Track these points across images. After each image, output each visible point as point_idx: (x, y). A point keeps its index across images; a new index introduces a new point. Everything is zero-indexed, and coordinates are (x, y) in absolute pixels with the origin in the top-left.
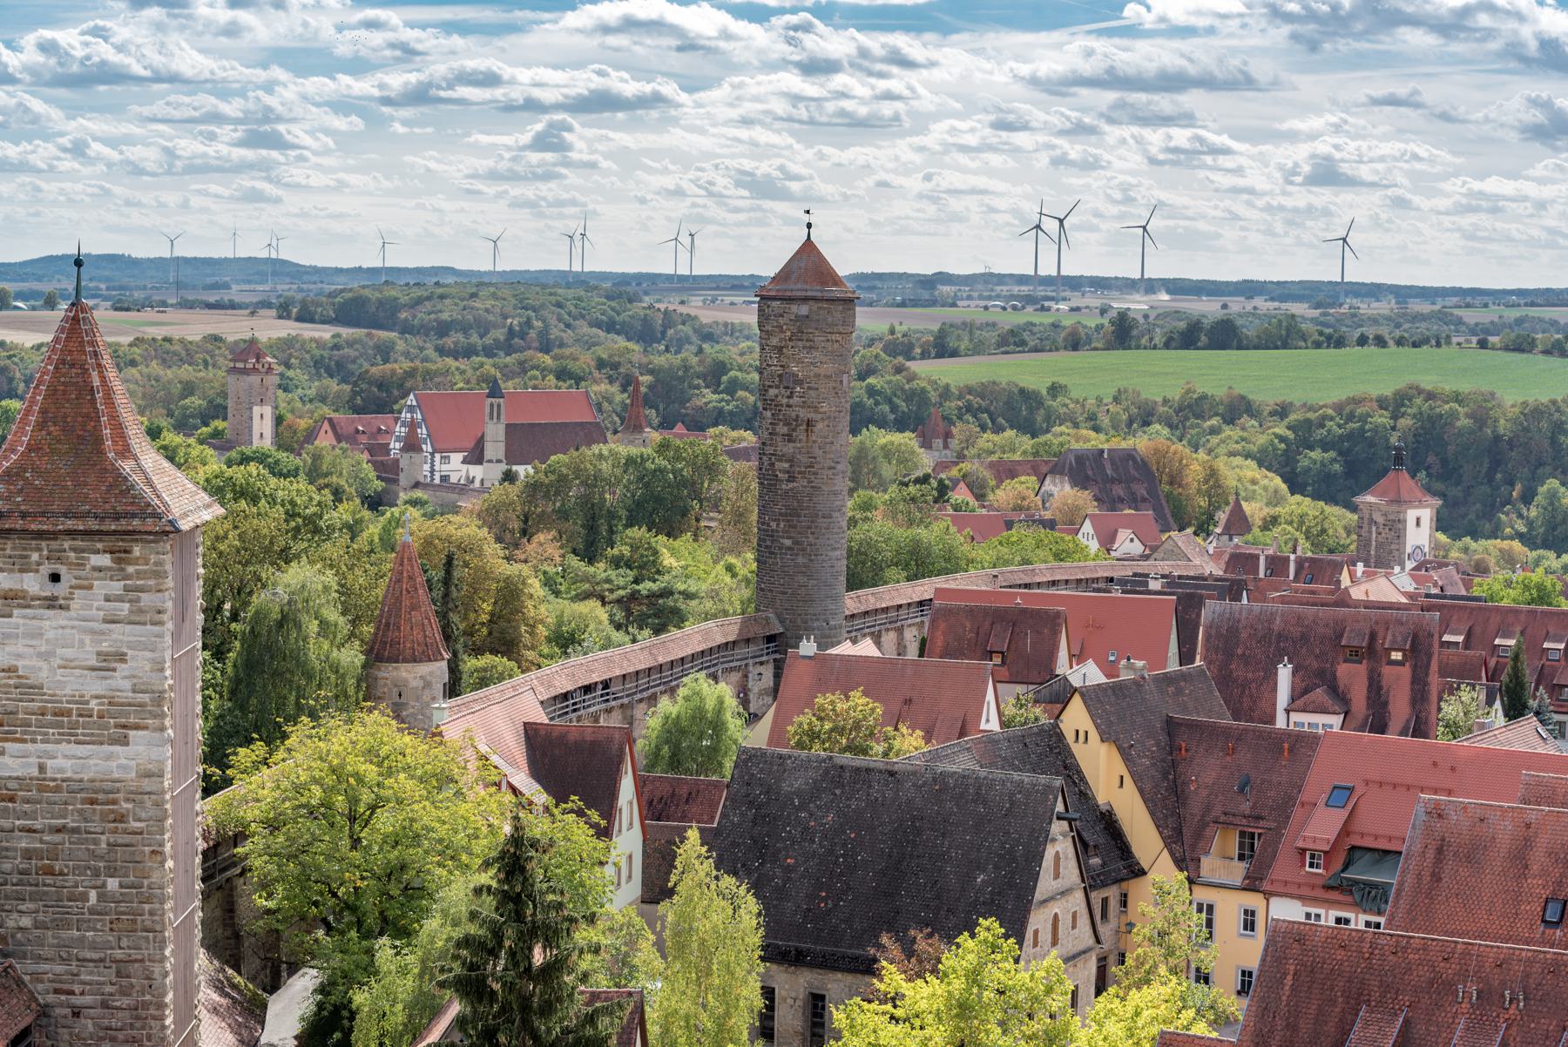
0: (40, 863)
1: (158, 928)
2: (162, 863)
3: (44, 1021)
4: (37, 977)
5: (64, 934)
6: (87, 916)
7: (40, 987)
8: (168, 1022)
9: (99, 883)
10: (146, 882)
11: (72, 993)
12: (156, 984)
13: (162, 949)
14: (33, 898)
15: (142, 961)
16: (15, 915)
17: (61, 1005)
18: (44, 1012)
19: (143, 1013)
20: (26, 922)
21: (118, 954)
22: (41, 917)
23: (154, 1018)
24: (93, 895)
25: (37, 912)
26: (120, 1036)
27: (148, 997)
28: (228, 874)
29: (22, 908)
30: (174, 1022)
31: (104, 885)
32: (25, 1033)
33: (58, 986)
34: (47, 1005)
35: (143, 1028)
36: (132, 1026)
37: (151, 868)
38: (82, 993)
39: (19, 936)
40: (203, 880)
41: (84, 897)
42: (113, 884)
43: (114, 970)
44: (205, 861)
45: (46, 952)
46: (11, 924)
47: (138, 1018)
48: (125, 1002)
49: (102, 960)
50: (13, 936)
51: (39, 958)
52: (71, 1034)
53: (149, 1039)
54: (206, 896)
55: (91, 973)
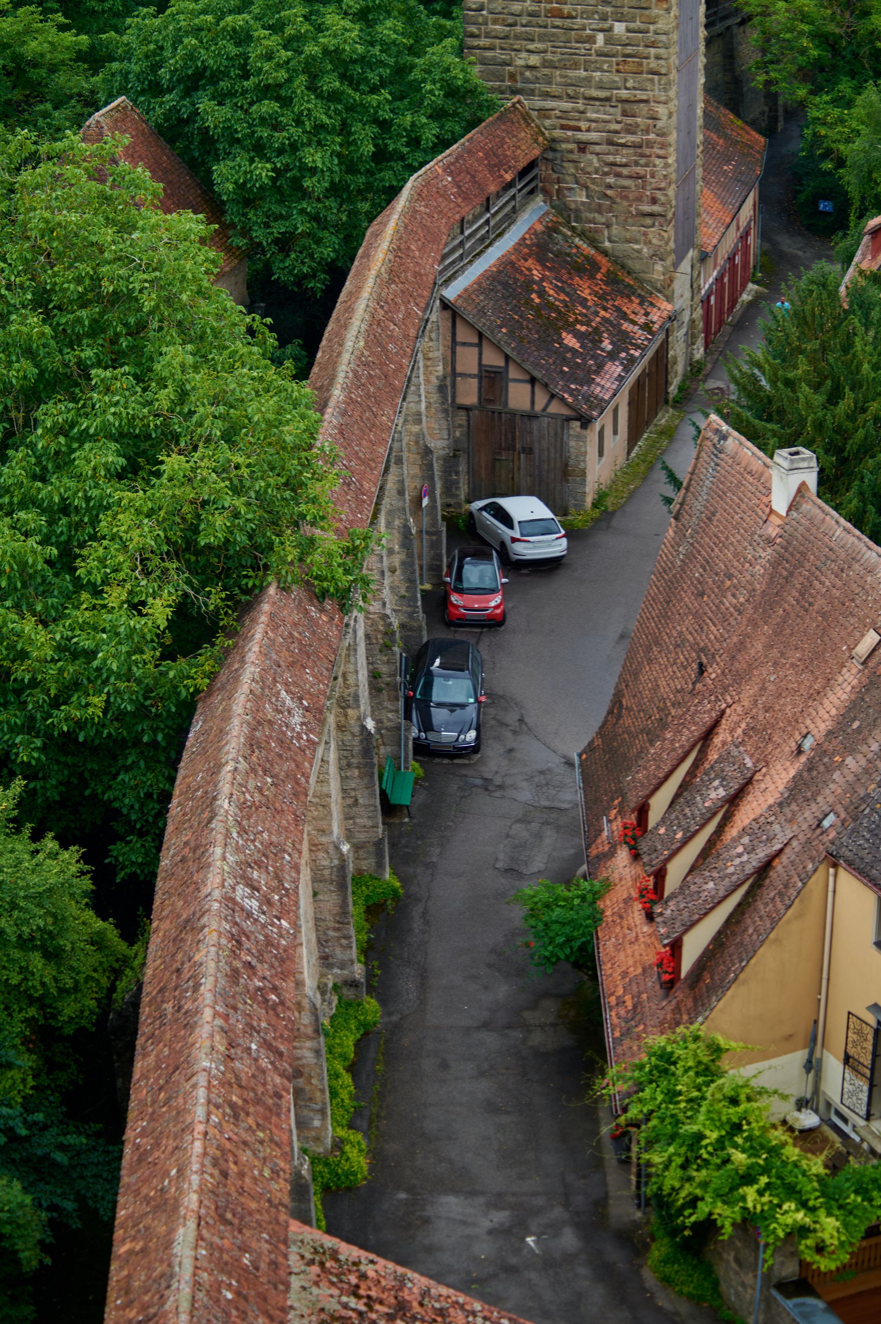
0: (548, 6)
1: (663, 71)
2: (668, 10)
3: (550, 155)
4: (544, 113)
5: (570, 73)
6: (594, 58)
7: (548, 123)
8: (670, 161)
9: (606, 26)
10: (652, 27)
11: (578, 129)
12: (660, 124)
13: (665, 90)
14: (542, 38)
15: (646, 101)
16: (524, 55)
17: (567, 140)
18: (552, 145)
19: (647, 151)
20: (534, 60)
21: (624, 93)
22: (549, 56)
23: (659, 157)
24: (600, 38)
25: (545, 51)
26: (625, 171)
27: (652, 136)
28: (729, 22)
29: (531, 47)
30: (677, 161)
31: (610, 29)
32: (532, 165)
33: (564, 122)
34: (554, 140)
35: (647, 165)
36: (637, 164)
37: (657, 16)
38: (588, 130)
39: (528, 74)
40: (707, 26)
41: (591, 40)
42: (619, 28)
43: (619, 110)
44: (708, 9)
45: (554, 89)
46: (520, 62)
47: (642, 155)
48: (631, 138)
49: (608, 99)
50: (522, 74)
51: (547, 95)
52: (576, 168)
53: (653, 177)
54: (709, 42)
55: (597, 112)
